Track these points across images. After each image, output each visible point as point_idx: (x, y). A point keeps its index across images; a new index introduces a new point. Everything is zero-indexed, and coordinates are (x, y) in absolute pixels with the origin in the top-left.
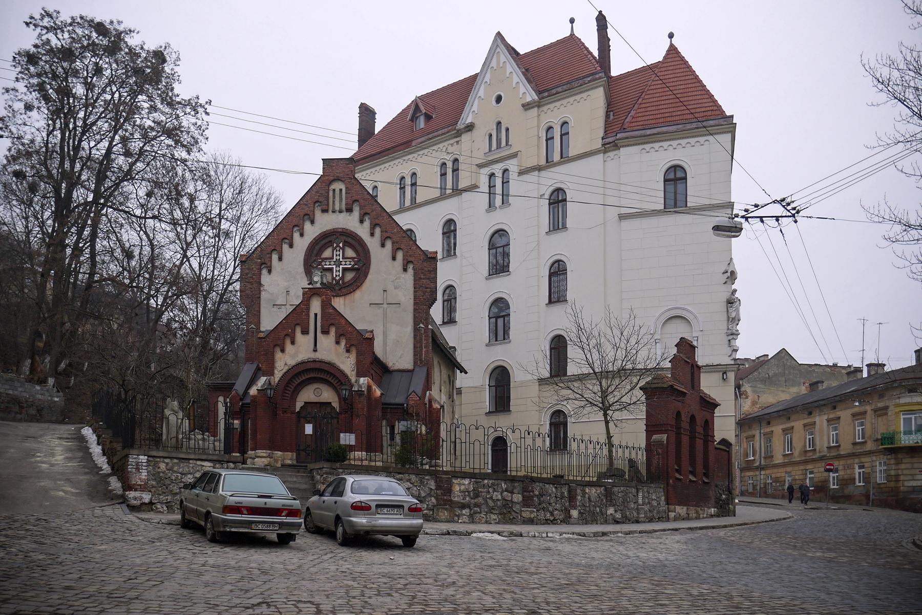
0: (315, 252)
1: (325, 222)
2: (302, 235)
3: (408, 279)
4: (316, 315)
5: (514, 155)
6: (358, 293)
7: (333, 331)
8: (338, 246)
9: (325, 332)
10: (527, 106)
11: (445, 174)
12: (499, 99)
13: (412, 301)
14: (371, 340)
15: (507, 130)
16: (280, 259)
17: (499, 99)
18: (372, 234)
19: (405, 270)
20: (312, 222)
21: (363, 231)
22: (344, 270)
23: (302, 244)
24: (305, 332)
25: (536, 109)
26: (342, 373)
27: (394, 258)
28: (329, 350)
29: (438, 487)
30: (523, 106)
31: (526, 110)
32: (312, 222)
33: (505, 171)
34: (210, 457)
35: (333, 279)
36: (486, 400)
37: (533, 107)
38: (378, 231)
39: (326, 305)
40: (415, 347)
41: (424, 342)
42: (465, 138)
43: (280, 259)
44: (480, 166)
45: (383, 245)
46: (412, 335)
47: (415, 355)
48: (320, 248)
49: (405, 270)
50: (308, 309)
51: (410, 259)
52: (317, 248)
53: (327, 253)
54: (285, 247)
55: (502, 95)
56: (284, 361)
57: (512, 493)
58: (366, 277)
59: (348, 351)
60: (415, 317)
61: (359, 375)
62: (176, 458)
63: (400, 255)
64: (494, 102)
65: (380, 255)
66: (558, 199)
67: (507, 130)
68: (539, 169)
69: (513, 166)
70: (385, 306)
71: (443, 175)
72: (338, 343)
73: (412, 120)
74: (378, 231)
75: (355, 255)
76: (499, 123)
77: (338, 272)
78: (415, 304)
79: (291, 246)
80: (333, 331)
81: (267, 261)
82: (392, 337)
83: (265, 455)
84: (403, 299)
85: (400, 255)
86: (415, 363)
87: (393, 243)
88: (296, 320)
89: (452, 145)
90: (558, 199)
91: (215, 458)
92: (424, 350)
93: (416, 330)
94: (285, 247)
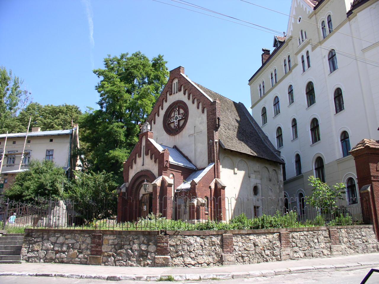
1: (171, 99)
3: (204, 117)
5: (308, 43)
6: (184, 130)
8: (176, 109)
9: (147, 154)
10: (310, 17)
18: (189, 99)
19: (203, 112)
20: (166, 101)
22: (179, 121)
25: (314, 16)
26: (153, 174)
27: (198, 108)
29: (93, 242)
30: (308, 17)
31: (310, 18)
33: (308, 52)
37: (313, 16)
42: (290, 43)
44: (297, 54)
45: (193, 103)
47: (209, 158)
48: (170, 113)
53: (173, 115)
55: (300, 17)
56: (132, 174)
57: (148, 245)
59: (155, 162)
60: (208, 137)
65: (192, 108)
66: (332, 57)
68: (320, 43)
69: (309, 48)
70: (195, 134)
72: (151, 158)
76: (302, 31)
77: (176, 124)
78: (208, 129)
82: (199, 150)
84: (203, 129)
90: (332, 57)
93: (208, 144)
94: (157, 116)
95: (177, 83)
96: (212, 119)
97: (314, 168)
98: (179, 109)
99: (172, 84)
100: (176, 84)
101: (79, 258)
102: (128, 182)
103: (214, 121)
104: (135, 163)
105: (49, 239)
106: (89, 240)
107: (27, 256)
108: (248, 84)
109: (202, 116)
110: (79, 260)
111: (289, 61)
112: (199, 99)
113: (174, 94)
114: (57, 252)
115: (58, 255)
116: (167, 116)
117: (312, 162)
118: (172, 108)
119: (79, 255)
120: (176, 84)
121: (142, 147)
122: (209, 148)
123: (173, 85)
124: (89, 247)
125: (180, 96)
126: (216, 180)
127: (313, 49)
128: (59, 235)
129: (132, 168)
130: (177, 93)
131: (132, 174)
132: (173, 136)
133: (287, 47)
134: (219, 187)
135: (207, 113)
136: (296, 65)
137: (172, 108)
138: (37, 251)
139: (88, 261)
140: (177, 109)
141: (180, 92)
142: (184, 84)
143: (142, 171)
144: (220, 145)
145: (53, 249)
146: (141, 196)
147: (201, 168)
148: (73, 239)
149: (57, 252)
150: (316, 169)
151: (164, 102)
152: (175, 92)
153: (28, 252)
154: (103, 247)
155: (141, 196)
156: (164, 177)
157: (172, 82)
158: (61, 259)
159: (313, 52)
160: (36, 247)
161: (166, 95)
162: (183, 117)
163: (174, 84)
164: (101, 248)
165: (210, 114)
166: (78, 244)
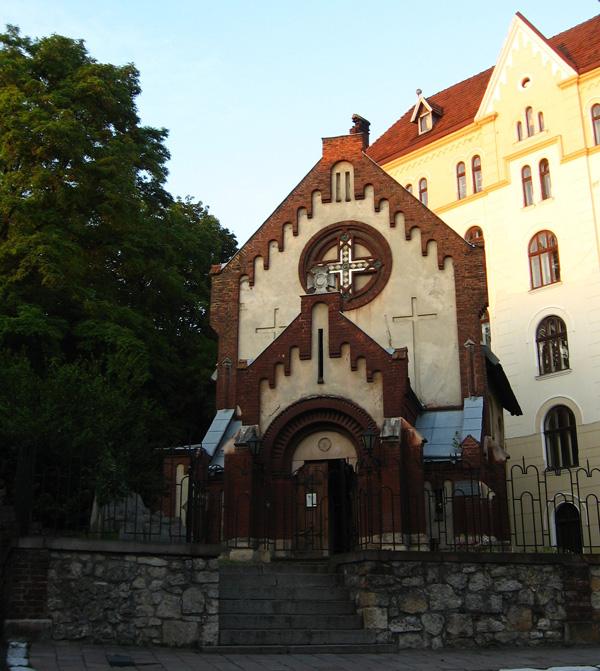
0: (314, 255)
1: (327, 214)
2: (296, 234)
3: (447, 280)
4: (321, 331)
5: (552, 141)
7: (347, 351)
8: (345, 244)
9: (336, 354)
10: (564, 85)
11: (463, 174)
12: (527, 80)
14: (401, 359)
15: (540, 114)
16: (267, 267)
17: (527, 80)
18: (393, 225)
19: (441, 267)
20: (310, 216)
21: (380, 222)
22: (355, 275)
23: (295, 245)
24: (306, 356)
26: (363, 411)
27: (425, 253)
28: (344, 381)
30: (559, 86)
31: (563, 88)
32: (310, 216)
33: (544, 163)
34: (163, 549)
35: (340, 287)
36: (541, 454)
38: (400, 219)
39: (335, 318)
40: (462, 373)
42: (488, 128)
43: (267, 267)
44: (509, 159)
45: (408, 238)
46: (457, 357)
47: (463, 384)
48: (320, 251)
49: (441, 267)
50: (310, 323)
51: (447, 253)
52: (317, 249)
53: (331, 254)
58: (386, 281)
59: (370, 379)
60: (460, 331)
61: (388, 414)
62: (101, 553)
63: (433, 249)
64: (520, 84)
67: (540, 114)
70: (415, 319)
71: (461, 175)
72: (354, 368)
73: (416, 122)
74: (400, 219)
75: (369, 254)
76: (529, 108)
77: (346, 279)
78: (459, 312)
79: (281, 249)
80: (347, 351)
81: (248, 270)
83: (245, 545)
84: (440, 307)
85: (433, 249)
86: (464, 396)
87: (422, 234)
88: (293, 341)
89: (470, 140)
91: (173, 549)
93: (461, 348)
94: (274, 250)
95: (347, 174)
96: (474, 289)
97: (542, 431)
98: (354, 243)
99: (331, 175)
100: (343, 177)
101: (540, 630)
102: (258, 421)
103: (480, 294)
104: (288, 373)
105: (448, 579)
106: (555, 582)
107: (389, 630)
109: (437, 275)
110: (542, 635)
111: (476, 169)
112: (428, 232)
114: (477, 616)
115: (481, 625)
116: (309, 256)
117: (538, 415)
118: (333, 236)
119: (537, 622)
120: (343, 177)
121: (315, 333)
122: (467, 360)
123: (334, 178)
124: (559, 598)
125: (362, 211)
127: (565, 159)
128: (472, 569)
129: (273, 386)
130: (348, 200)
131: (275, 402)
133: (478, 132)
135: (456, 271)
136: (504, 183)
137: (329, 238)
138: (418, 615)
139: (567, 638)
140: (350, 243)
141: (358, 202)
142: (377, 184)
143: (320, 397)
145: (462, 610)
146: (297, 465)
147: (435, 406)
148: (513, 578)
149: (477, 616)
150: (546, 433)
152: (343, 196)
153: (390, 619)
154: (594, 598)
155: (297, 465)
157: (332, 169)
158: (491, 635)
159: (564, 165)
160: (410, 606)
161: (309, 200)
162: (370, 266)
163: (338, 174)
164: (589, 601)
165: (467, 275)
166: (529, 591)
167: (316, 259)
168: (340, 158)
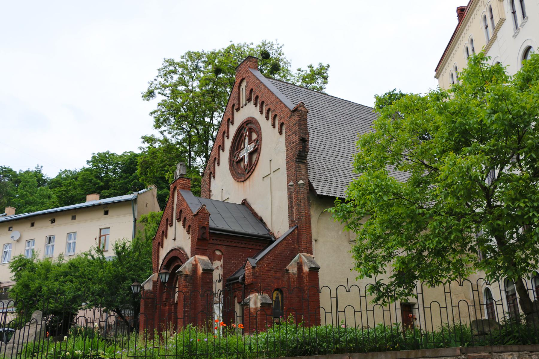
1: (240, 118)
6: (256, 170)
13: (285, 162)
18: (261, 112)
41: (294, 200)
45: (267, 118)
54: (221, 151)
59: (188, 232)
60: (288, 177)
78: (288, 162)
92: (295, 208)
94: (221, 151)
96: (293, 143)
108: (435, 77)
113: (242, 107)
116: (234, 148)
126: (300, 257)
130: (246, 105)
132: (242, 183)
134: (306, 269)
136: (502, 21)
144: (311, 189)
151: (231, 126)
156: (197, 256)
167: (237, 150)
168: (241, 78)
